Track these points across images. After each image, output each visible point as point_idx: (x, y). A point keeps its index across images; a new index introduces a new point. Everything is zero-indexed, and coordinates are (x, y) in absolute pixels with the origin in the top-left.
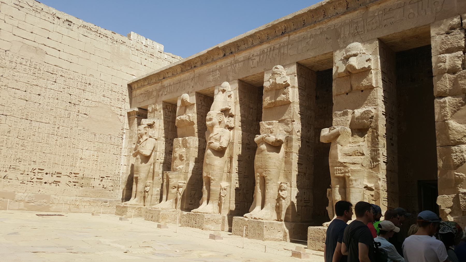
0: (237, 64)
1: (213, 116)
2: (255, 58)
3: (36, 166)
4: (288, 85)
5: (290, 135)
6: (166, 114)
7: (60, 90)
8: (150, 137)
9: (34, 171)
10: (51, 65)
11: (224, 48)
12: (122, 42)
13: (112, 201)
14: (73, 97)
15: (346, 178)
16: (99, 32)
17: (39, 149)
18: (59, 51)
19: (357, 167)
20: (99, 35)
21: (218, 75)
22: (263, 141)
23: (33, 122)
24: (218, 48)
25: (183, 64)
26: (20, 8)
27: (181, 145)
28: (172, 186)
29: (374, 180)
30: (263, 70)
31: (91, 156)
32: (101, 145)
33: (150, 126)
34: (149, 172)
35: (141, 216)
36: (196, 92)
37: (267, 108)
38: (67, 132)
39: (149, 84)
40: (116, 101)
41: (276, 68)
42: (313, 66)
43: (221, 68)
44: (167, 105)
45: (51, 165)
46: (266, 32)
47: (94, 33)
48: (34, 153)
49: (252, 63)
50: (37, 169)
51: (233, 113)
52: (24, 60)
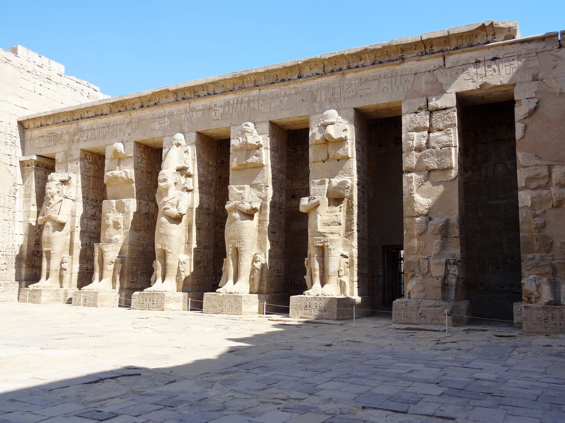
0: (194, 113)
1: (167, 177)
2: (218, 108)
4: (261, 146)
5: (264, 201)
6: (85, 166)
8: (66, 197)
11: (175, 92)
12: (5, 60)
13: (7, 284)
15: (325, 248)
19: (335, 237)
21: (167, 124)
22: (236, 208)
24: (168, 90)
25: (113, 104)
27: (115, 209)
28: (108, 262)
29: (349, 248)
30: (229, 125)
33: (64, 182)
34: (65, 243)
35: (59, 301)
36: (135, 142)
37: (234, 169)
39: (54, 123)
41: (247, 125)
42: (285, 126)
43: (171, 115)
44: (86, 155)
46: (232, 81)
49: (214, 115)
51: (192, 173)
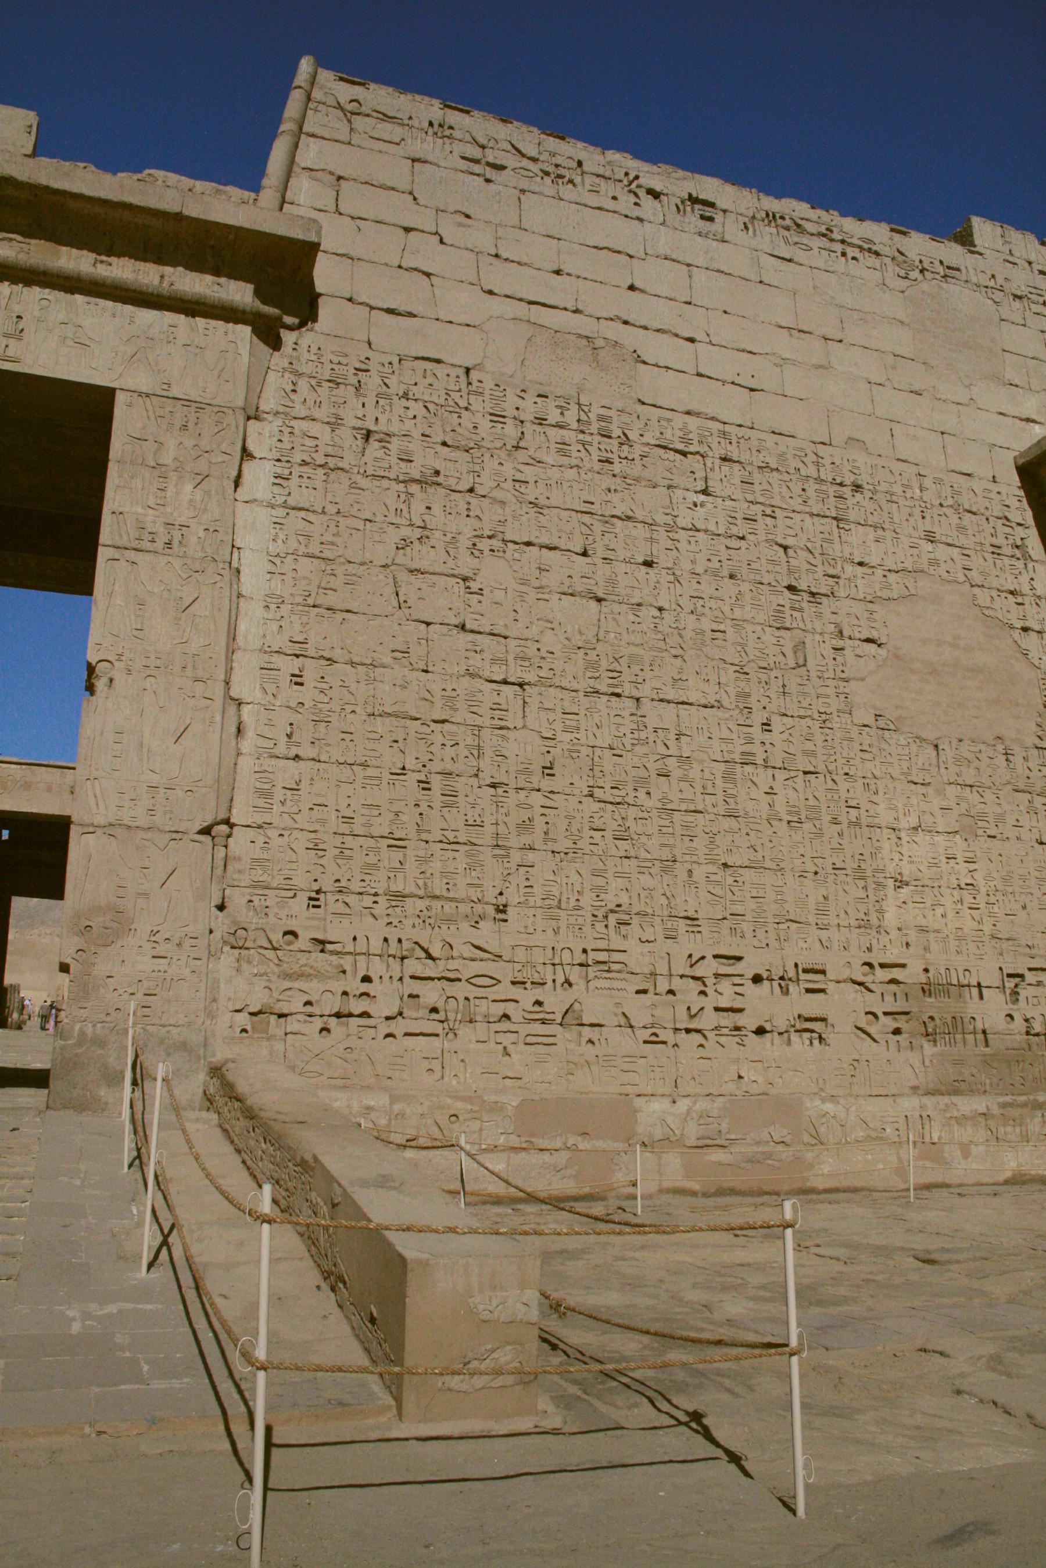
3: (703, 944)
7: (734, 530)
9: (698, 974)
10: (669, 415)
14: (800, 559)
16: (836, 236)
17: (700, 844)
18: (692, 340)
20: (838, 247)
23: (647, 706)
26: (490, 173)
31: (943, 865)
32: (973, 797)
38: (809, 746)
40: (989, 556)
45: (771, 927)
47: (816, 243)
48: (681, 870)
50: (709, 957)
52: (551, 403)
